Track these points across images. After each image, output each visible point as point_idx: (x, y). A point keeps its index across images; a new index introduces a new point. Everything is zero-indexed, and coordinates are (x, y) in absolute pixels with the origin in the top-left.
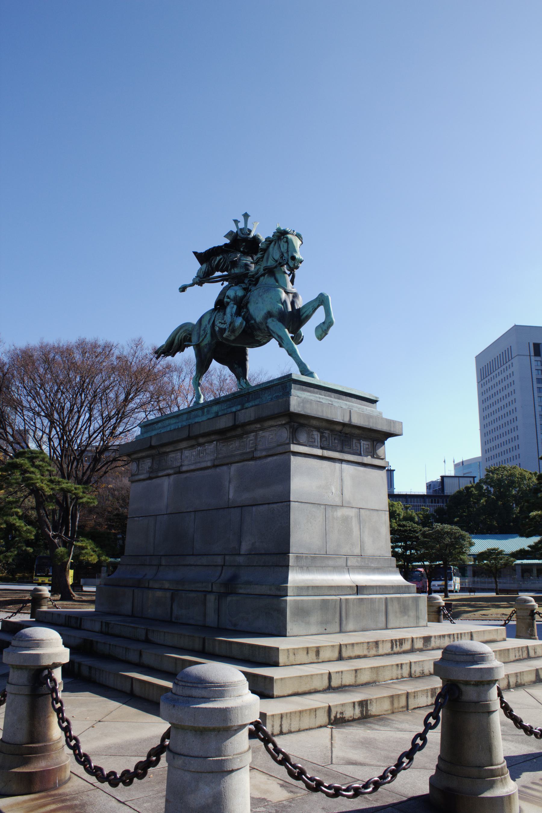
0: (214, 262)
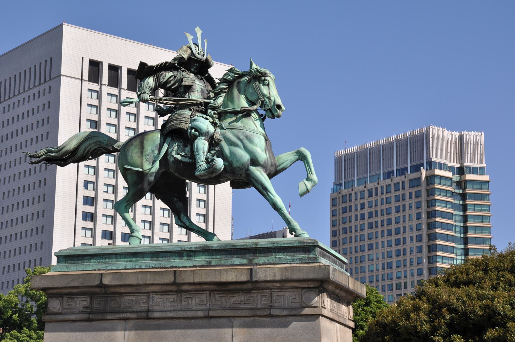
0: (163, 78)
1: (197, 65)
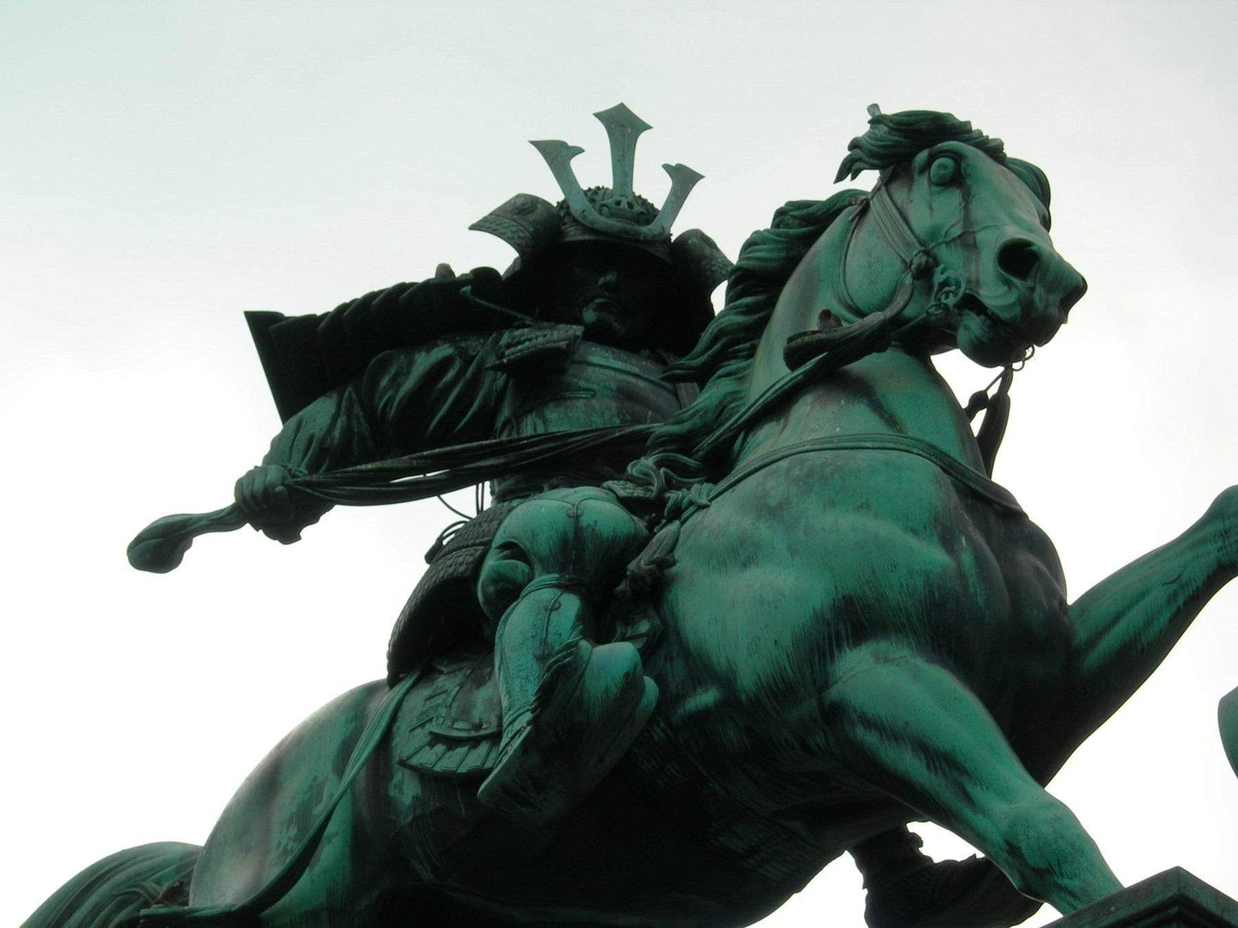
0: (395, 383)
1: (610, 277)
